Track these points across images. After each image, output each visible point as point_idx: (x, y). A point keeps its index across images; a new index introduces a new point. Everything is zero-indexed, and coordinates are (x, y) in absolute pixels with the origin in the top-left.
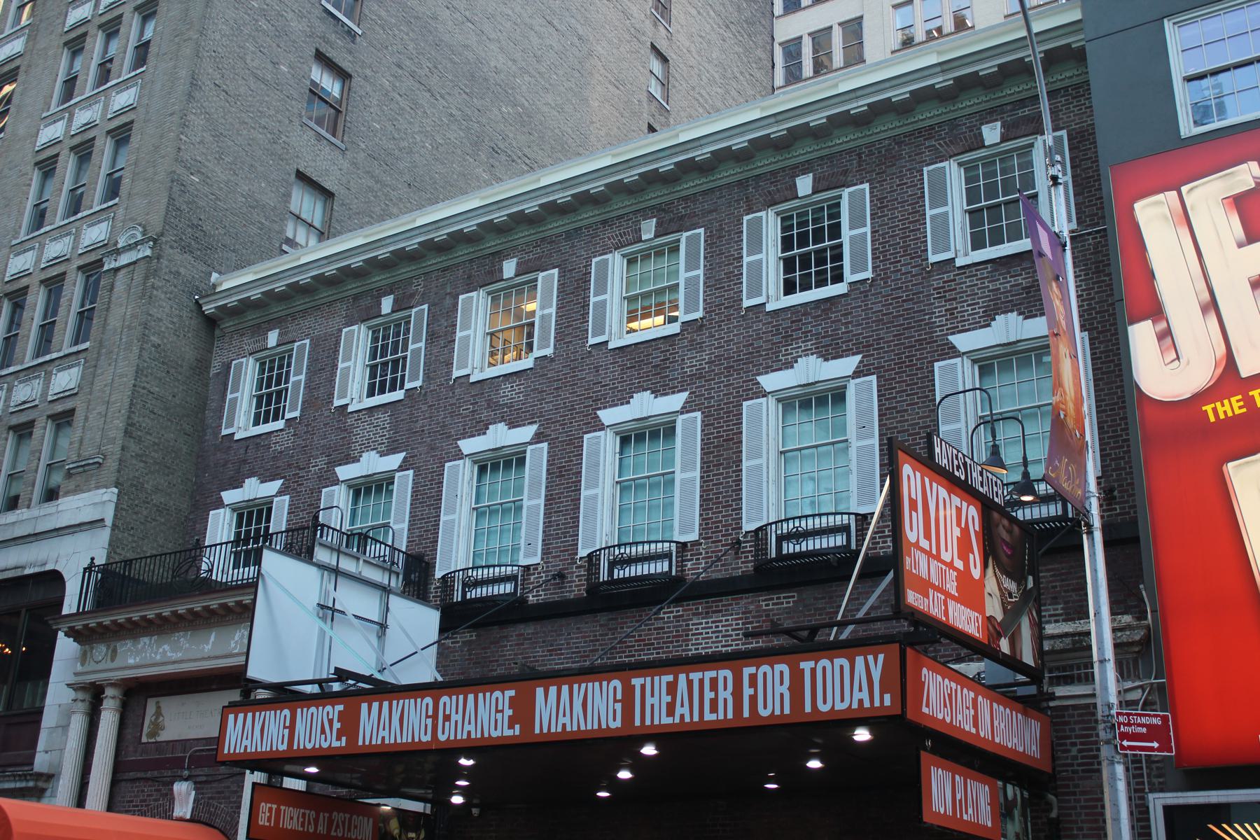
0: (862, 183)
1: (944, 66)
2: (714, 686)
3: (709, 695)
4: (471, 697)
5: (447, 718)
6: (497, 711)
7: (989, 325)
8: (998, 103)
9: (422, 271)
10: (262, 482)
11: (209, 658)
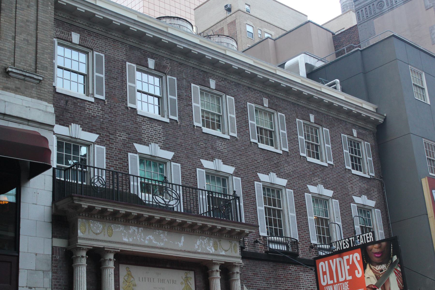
7: (360, 197)
8: (355, 124)
9: (170, 57)
10: (83, 130)
11: (185, 251)
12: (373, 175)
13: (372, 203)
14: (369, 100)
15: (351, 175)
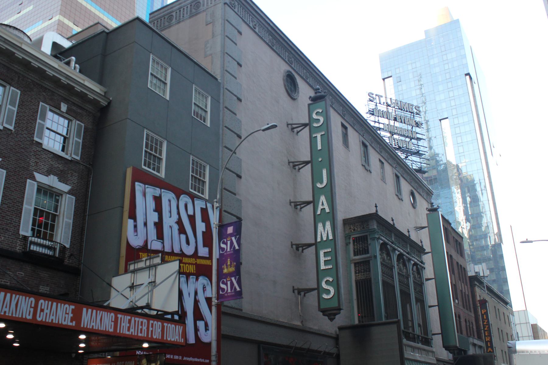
0: (17, 89)
1: (68, 77)
2: (142, 325)
3: (140, 327)
4: (55, 304)
5: (42, 310)
6: (66, 313)
7: (47, 176)
12: (78, 158)
13: (65, 188)
14: (100, 82)
15: (40, 149)
